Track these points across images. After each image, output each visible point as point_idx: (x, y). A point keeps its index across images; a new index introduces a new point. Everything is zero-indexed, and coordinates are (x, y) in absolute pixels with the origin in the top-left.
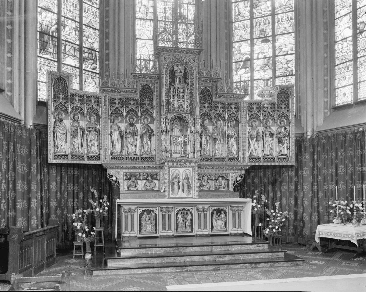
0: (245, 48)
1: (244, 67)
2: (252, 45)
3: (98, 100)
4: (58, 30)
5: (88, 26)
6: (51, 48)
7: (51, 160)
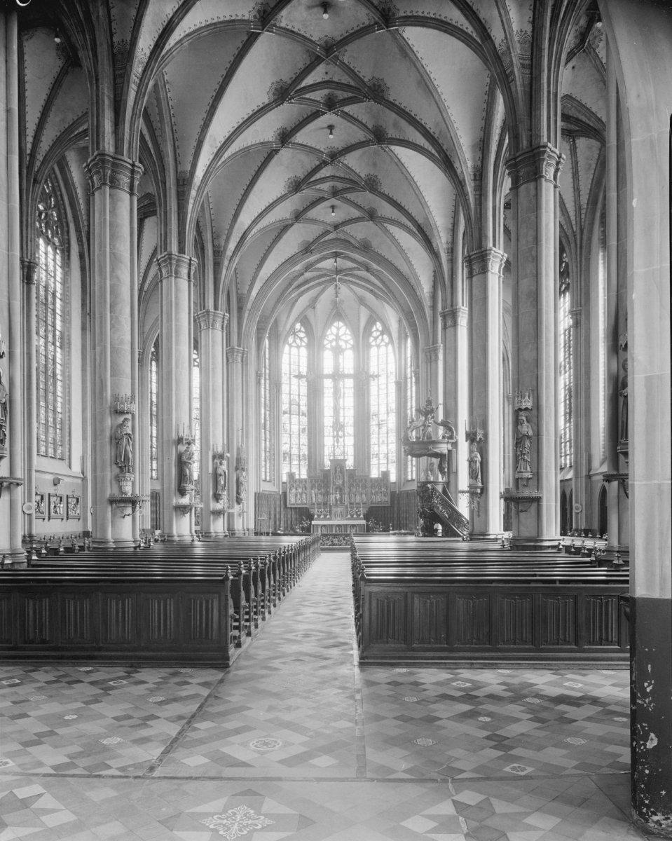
0: (376, 448)
1: (376, 457)
2: (379, 446)
3: (306, 482)
4: (290, 451)
5: (302, 445)
6: (288, 459)
7: (288, 506)
